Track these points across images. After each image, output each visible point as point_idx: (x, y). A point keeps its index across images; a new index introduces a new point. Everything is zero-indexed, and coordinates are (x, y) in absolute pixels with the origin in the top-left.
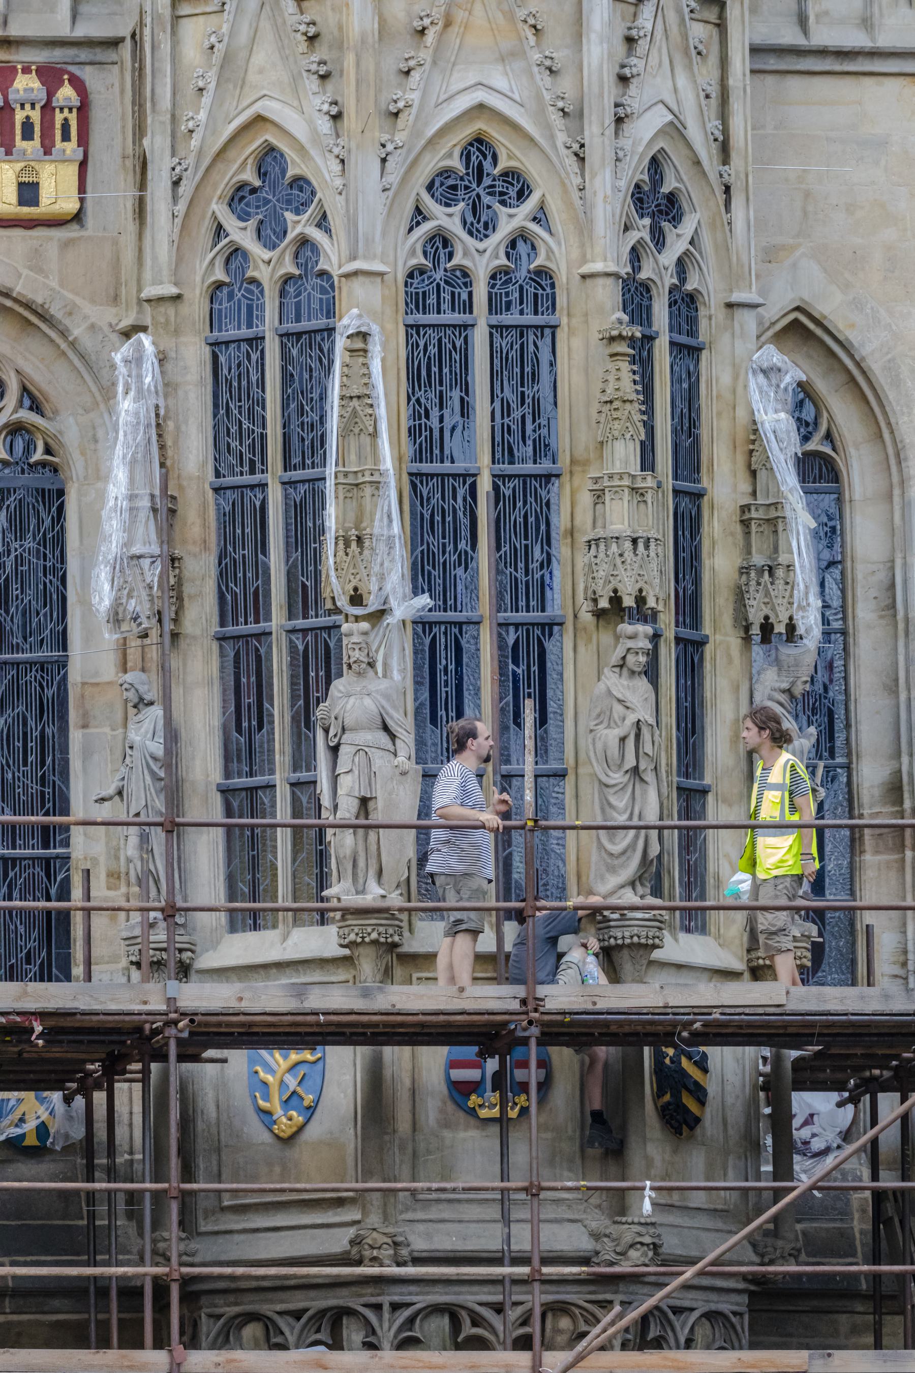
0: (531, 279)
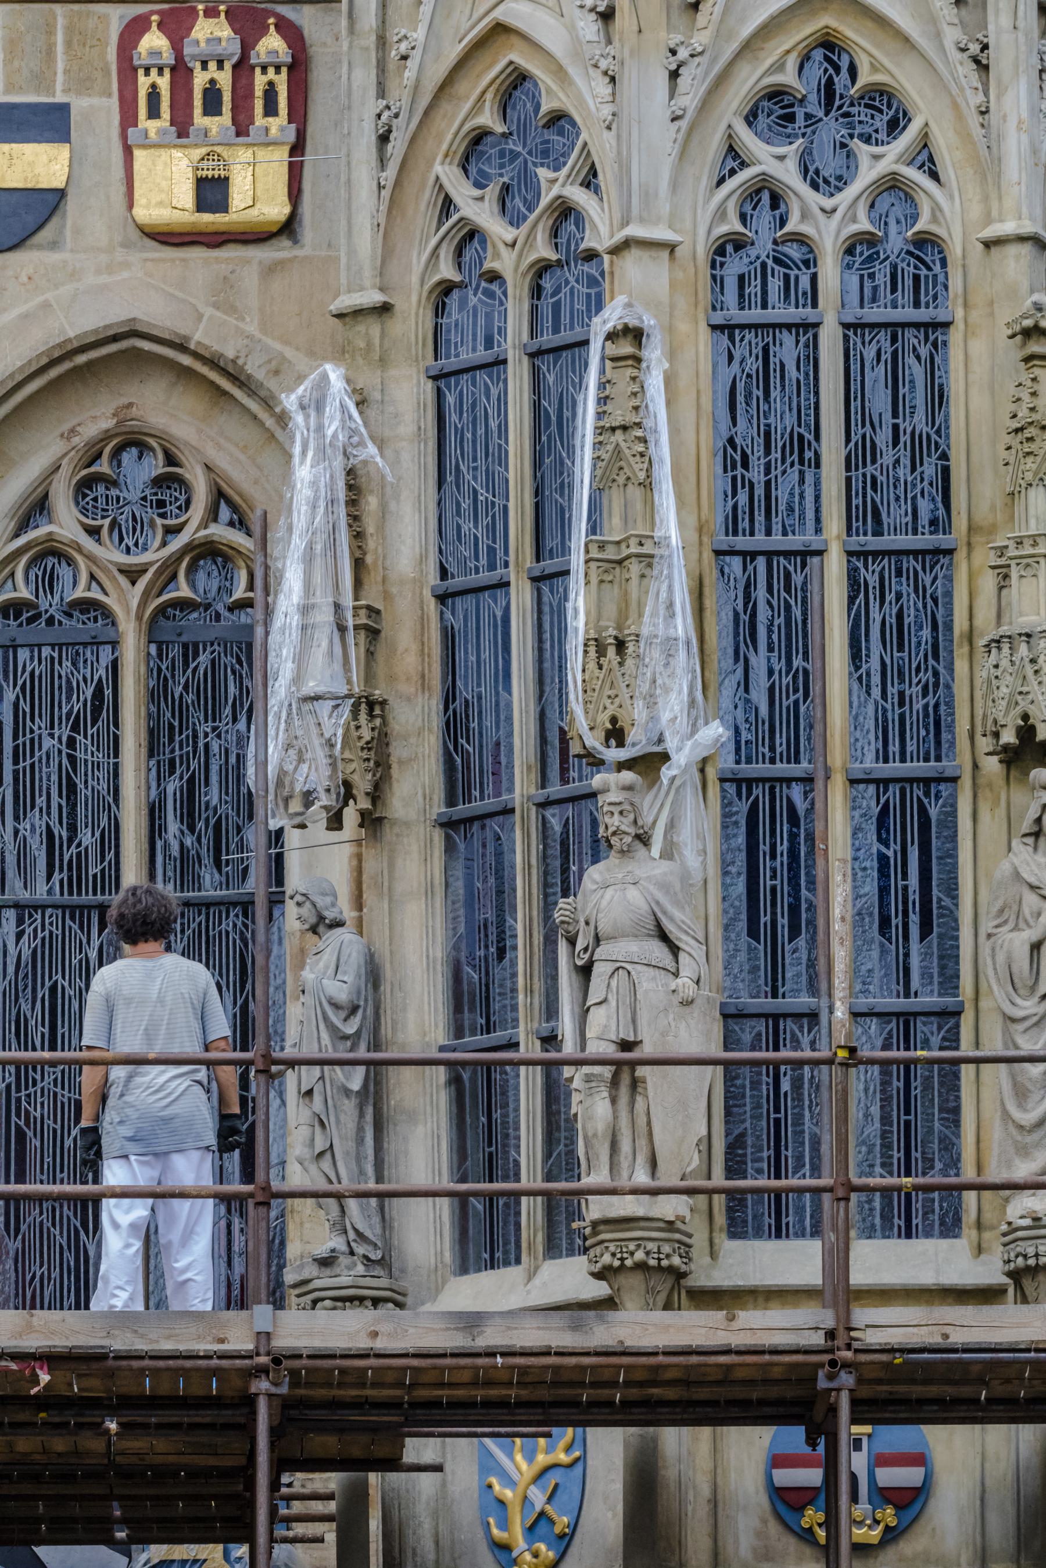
0: (908, 252)
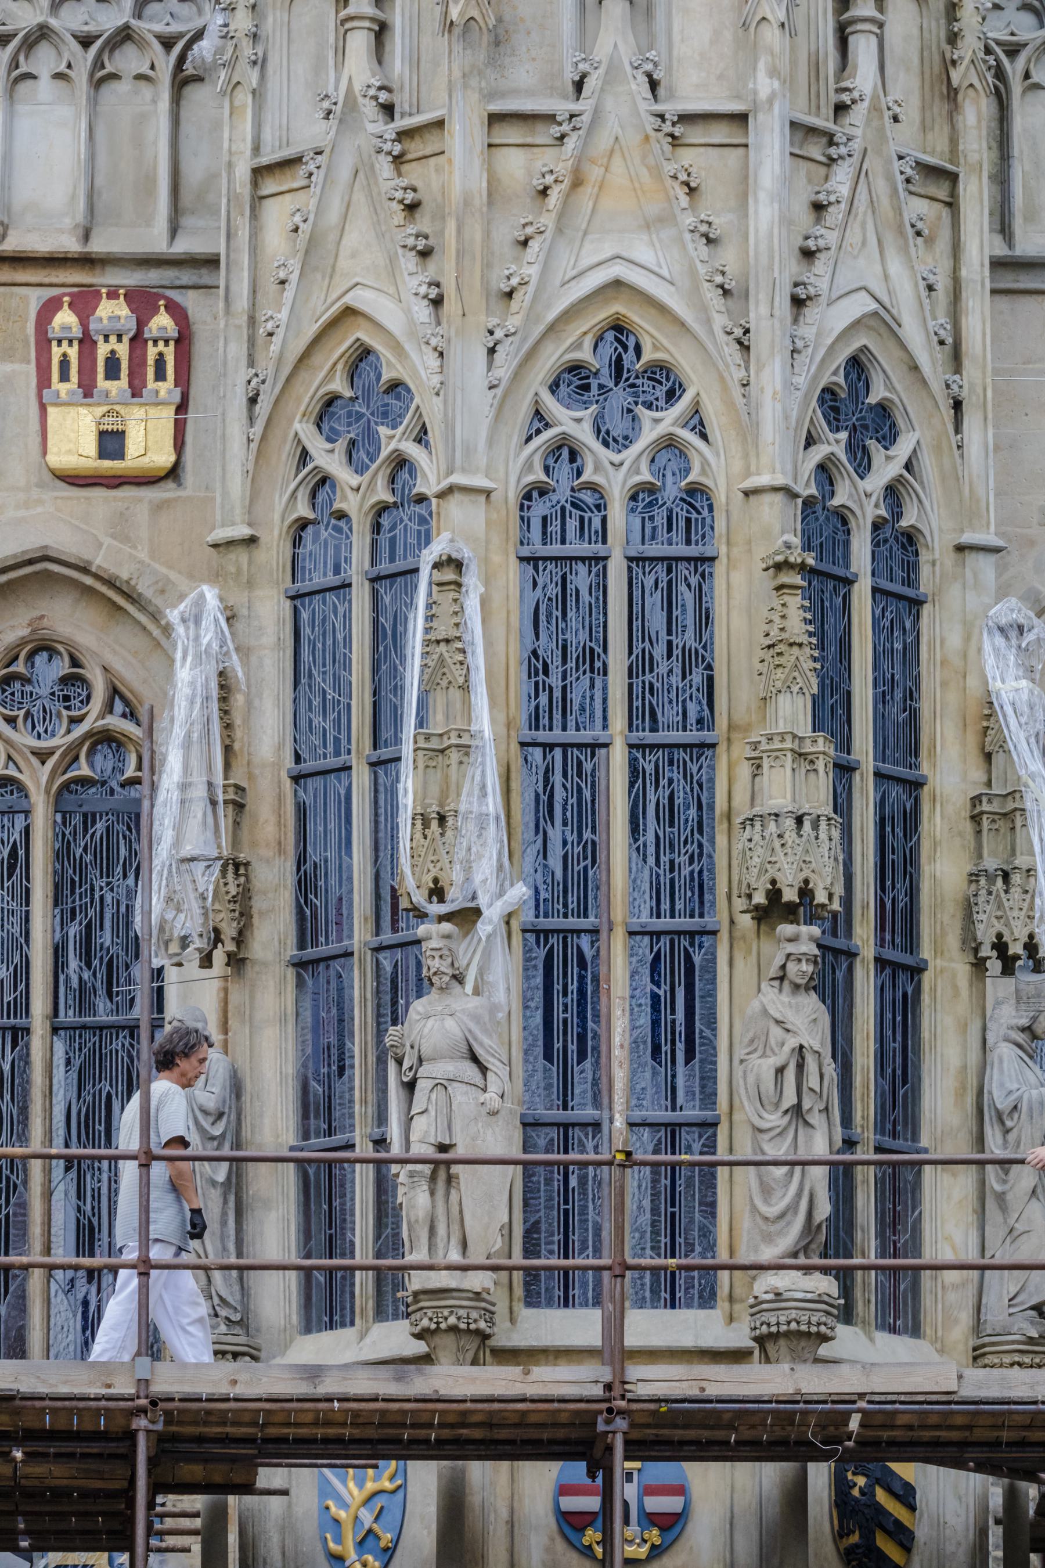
0: (682, 499)
